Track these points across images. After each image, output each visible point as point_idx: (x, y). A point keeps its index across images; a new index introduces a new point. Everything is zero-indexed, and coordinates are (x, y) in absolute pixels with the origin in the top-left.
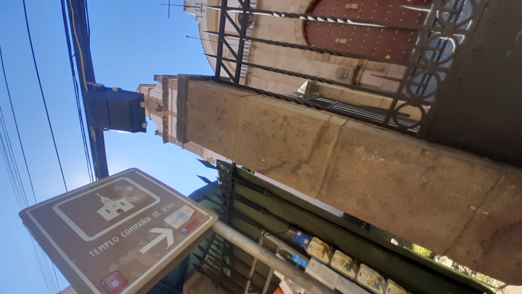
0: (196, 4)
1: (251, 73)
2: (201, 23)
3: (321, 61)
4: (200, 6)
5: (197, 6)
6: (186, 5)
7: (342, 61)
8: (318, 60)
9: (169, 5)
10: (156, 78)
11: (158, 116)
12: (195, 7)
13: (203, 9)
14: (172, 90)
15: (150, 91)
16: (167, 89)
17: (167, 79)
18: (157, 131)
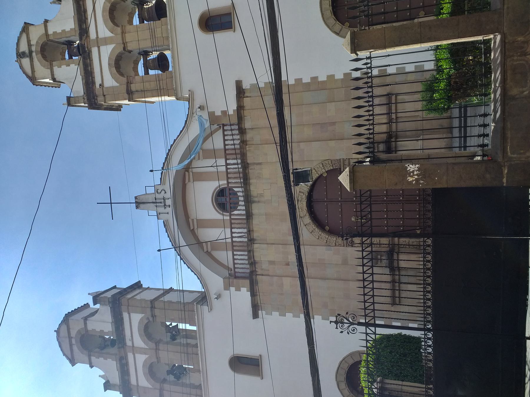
0: (156, 200)
1: (256, 271)
3: (344, 246)
4: (163, 201)
5: (157, 201)
8: (340, 245)
11: (106, 359)
13: (167, 204)
15: (87, 322)
16: (121, 314)
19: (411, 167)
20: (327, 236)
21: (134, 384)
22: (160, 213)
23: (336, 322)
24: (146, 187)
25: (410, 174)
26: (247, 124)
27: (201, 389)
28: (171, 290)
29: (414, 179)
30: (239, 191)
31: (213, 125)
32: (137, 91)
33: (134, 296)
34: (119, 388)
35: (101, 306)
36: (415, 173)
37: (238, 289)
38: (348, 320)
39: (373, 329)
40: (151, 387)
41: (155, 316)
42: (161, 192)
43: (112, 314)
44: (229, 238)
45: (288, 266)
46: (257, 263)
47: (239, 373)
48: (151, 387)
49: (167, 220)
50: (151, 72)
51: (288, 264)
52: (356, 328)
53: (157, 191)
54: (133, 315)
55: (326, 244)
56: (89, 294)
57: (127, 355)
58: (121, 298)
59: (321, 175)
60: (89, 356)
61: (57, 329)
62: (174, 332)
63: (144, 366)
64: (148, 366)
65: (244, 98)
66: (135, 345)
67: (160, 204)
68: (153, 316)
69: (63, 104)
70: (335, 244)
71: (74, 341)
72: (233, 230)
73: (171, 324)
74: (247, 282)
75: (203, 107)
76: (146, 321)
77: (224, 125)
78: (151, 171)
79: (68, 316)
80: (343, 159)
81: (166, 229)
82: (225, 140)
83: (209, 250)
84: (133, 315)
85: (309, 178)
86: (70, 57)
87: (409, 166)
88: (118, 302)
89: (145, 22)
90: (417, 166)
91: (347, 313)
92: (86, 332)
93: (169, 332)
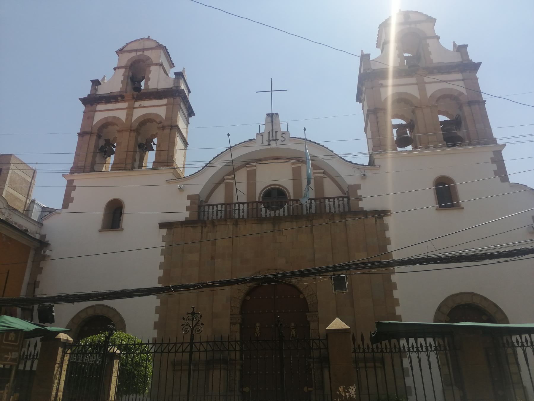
0: (275, 132)
1: (205, 227)
2: (256, 143)
3: (231, 315)
4: (274, 138)
5: (274, 133)
6: (274, 115)
9: (272, 91)
10: (180, 75)
11: (122, 82)
12: (272, 130)
13: (272, 143)
14: (166, 105)
15: (158, 66)
16: (165, 98)
18: (100, 84)
19: (352, 389)
20: (240, 298)
21: (97, 108)
22: (262, 135)
23: (193, 313)
24: (287, 123)
25: (346, 388)
26: (350, 221)
27: (90, 172)
28: (186, 145)
29: (341, 393)
30: (284, 211)
31: (348, 188)
32: (377, 118)
33: (182, 110)
34: (94, 94)
35: (173, 79)
36: (347, 394)
37: (188, 209)
38: (195, 325)
39: (188, 349)
40: (94, 124)
41: (163, 130)
42: (282, 137)
43: (166, 89)
44: (238, 200)
47: (106, 208)
48: (94, 124)
49: (256, 143)
50: (395, 130)
51: (212, 258)
52: (188, 332)
53: (284, 133)
54: (165, 108)
56: (184, 68)
57: (125, 102)
58: (181, 98)
59: (301, 292)
61: (150, 38)
62: (145, 146)
65: (374, 218)
66: (135, 110)
67: (271, 136)
68: (163, 128)
69: (362, 51)
70: (232, 305)
71: (140, 53)
72: (246, 205)
73: (154, 144)
74: (195, 217)
75: (365, 179)
76: (158, 121)
77: (348, 197)
78: (305, 129)
79: (164, 49)
80: (318, 315)
81: (247, 141)
82: (334, 198)
83: (226, 181)
84: (165, 108)
85: (339, 290)
86: (406, 58)
87: (354, 387)
88: (177, 95)
89: (441, 126)
90: (354, 396)
91: (202, 324)
92: (149, 65)
93: (146, 142)
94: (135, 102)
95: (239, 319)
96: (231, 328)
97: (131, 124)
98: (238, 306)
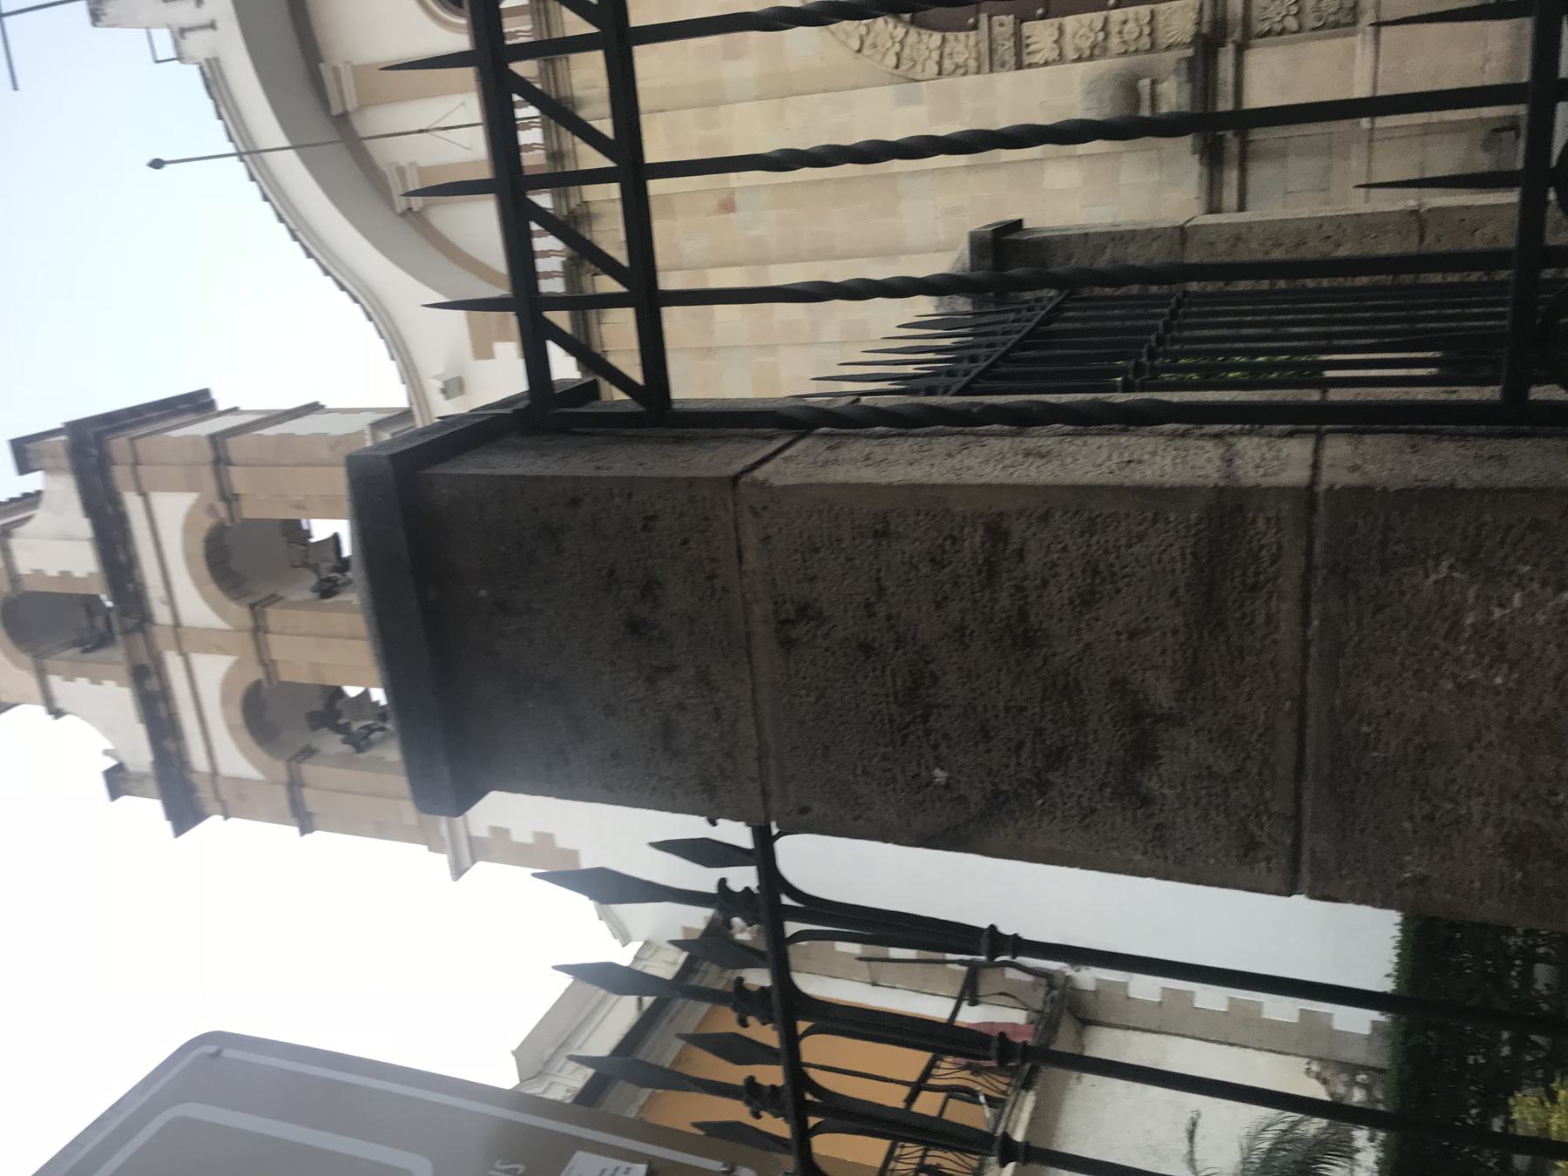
2: (217, 60)
3: (978, 73)
7: (1101, 36)
8: (961, 69)
11: (96, 681)
14: (143, 494)
16: (116, 501)
17: (99, 441)
20: (900, 31)
35: (49, 478)
41: (237, 496)
45: (731, 215)
46: (598, 216)
55: (895, 71)
60: (41, 674)
63: (225, 699)
64: (238, 698)
68: (228, 497)
70: (935, 69)
76: (208, 522)
88: (94, 452)
94: (155, 625)
95: (1002, 25)
96: (1042, 62)
97: (240, 631)
98: (937, 37)
